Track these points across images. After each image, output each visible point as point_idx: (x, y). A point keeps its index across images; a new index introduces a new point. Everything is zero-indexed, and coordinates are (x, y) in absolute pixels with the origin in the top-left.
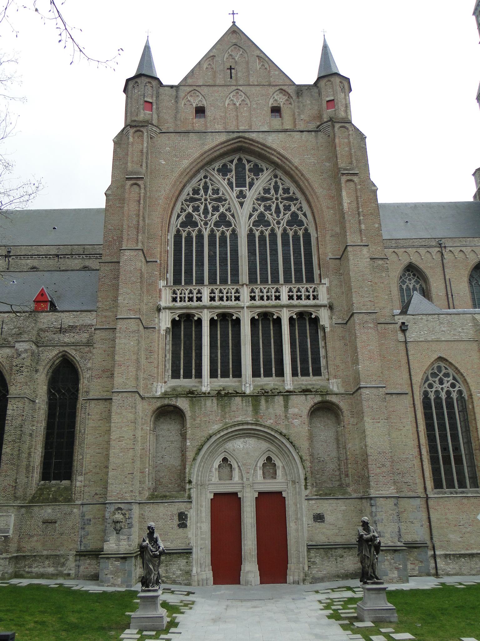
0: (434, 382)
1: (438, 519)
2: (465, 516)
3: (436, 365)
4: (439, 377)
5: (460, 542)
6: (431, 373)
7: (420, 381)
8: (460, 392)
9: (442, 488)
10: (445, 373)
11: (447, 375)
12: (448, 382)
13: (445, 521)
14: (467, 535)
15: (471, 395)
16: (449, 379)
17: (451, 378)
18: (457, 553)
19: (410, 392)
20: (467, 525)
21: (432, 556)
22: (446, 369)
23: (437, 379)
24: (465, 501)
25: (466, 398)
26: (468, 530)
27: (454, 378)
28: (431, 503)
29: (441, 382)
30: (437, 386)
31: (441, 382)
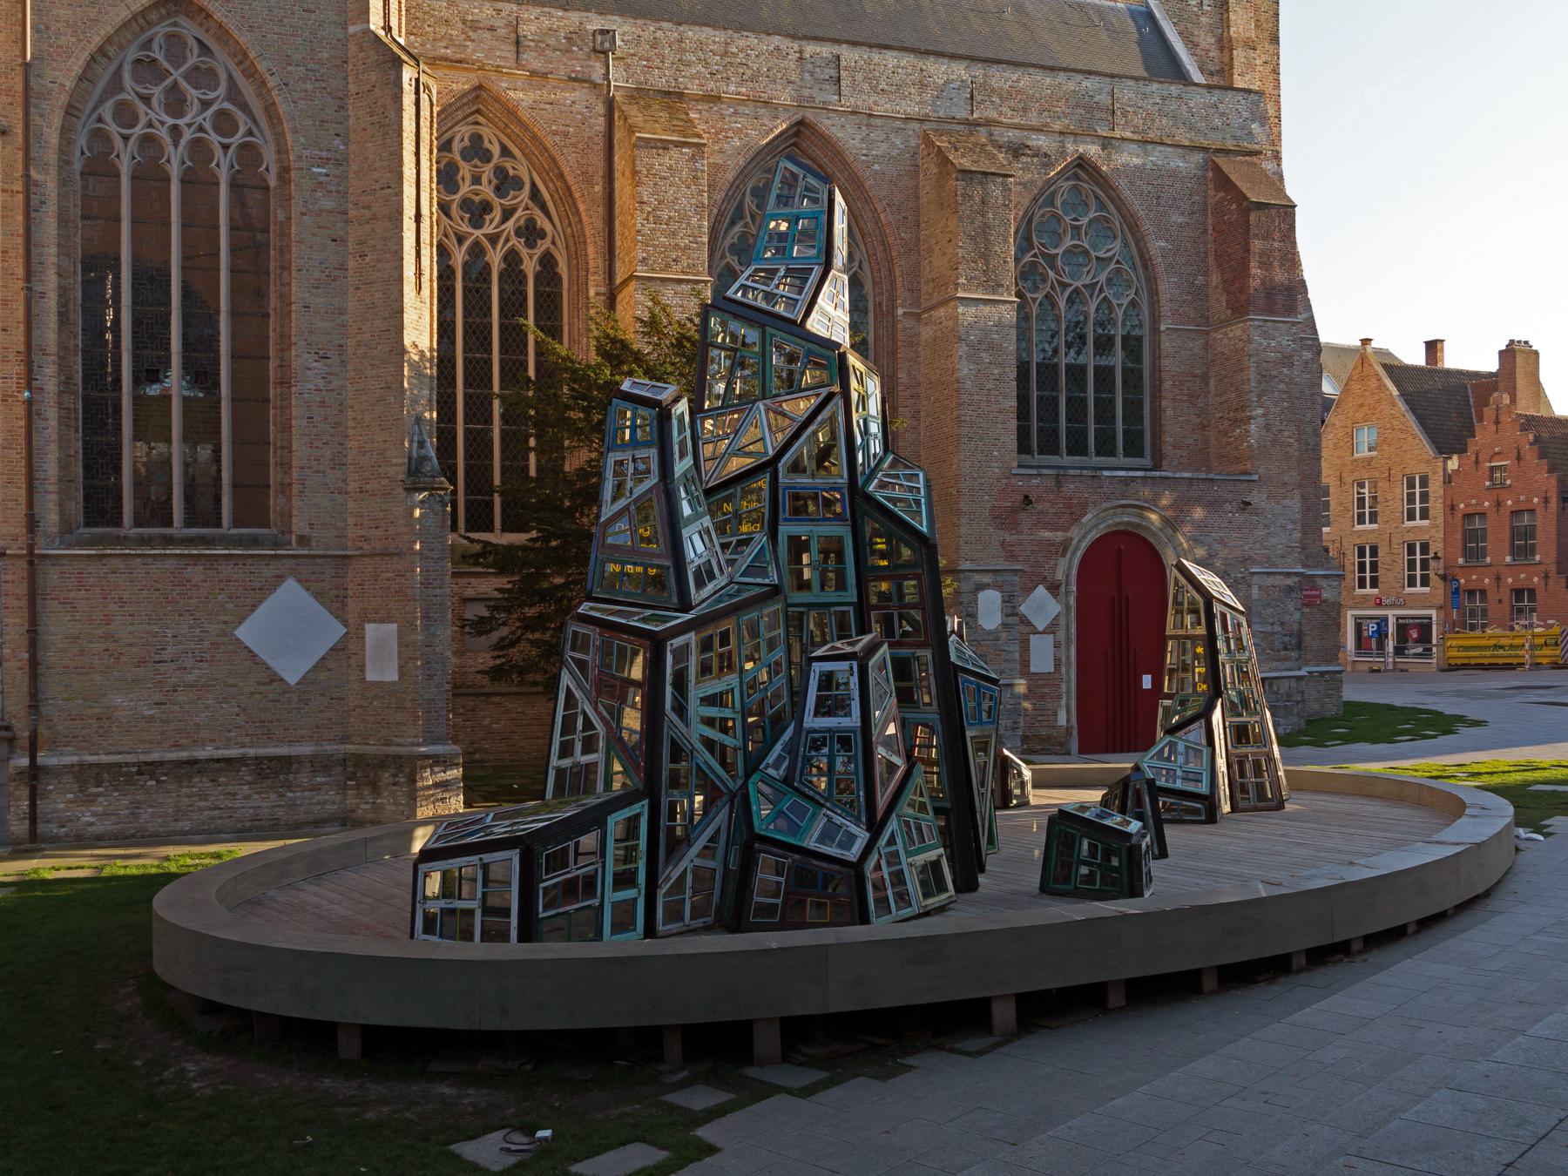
0: (146, 100)
1: (74, 639)
2: (184, 629)
3: (161, 30)
4: (184, 85)
5: (151, 719)
6: (138, 61)
7: (68, 84)
8: (248, 151)
9: (117, 521)
10: (196, 68)
11: (203, 76)
12: (206, 104)
13: (98, 647)
14: (181, 697)
15: (284, 171)
16: (212, 95)
17: (222, 90)
18: (130, 758)
19: (19, 130)
20: (189, 662)
21: (20, 773)
22: (204, 49)
23: (157, 92)
24: (196, 573)
25: (272, 183)
26: (190, 678)
27: (234, 94)
28: (51, 576)
29: (176, 103)
30: (155, 117)
31: (176, 103)
